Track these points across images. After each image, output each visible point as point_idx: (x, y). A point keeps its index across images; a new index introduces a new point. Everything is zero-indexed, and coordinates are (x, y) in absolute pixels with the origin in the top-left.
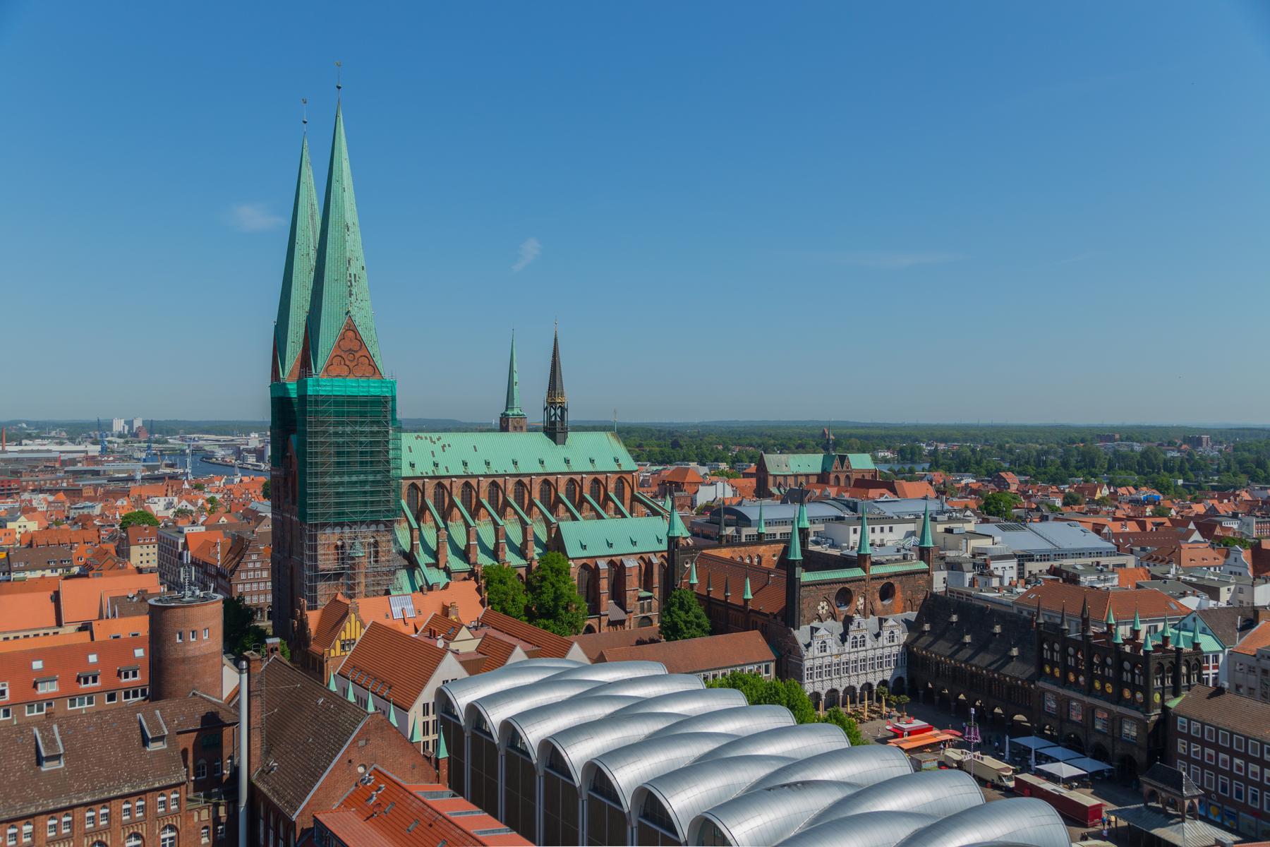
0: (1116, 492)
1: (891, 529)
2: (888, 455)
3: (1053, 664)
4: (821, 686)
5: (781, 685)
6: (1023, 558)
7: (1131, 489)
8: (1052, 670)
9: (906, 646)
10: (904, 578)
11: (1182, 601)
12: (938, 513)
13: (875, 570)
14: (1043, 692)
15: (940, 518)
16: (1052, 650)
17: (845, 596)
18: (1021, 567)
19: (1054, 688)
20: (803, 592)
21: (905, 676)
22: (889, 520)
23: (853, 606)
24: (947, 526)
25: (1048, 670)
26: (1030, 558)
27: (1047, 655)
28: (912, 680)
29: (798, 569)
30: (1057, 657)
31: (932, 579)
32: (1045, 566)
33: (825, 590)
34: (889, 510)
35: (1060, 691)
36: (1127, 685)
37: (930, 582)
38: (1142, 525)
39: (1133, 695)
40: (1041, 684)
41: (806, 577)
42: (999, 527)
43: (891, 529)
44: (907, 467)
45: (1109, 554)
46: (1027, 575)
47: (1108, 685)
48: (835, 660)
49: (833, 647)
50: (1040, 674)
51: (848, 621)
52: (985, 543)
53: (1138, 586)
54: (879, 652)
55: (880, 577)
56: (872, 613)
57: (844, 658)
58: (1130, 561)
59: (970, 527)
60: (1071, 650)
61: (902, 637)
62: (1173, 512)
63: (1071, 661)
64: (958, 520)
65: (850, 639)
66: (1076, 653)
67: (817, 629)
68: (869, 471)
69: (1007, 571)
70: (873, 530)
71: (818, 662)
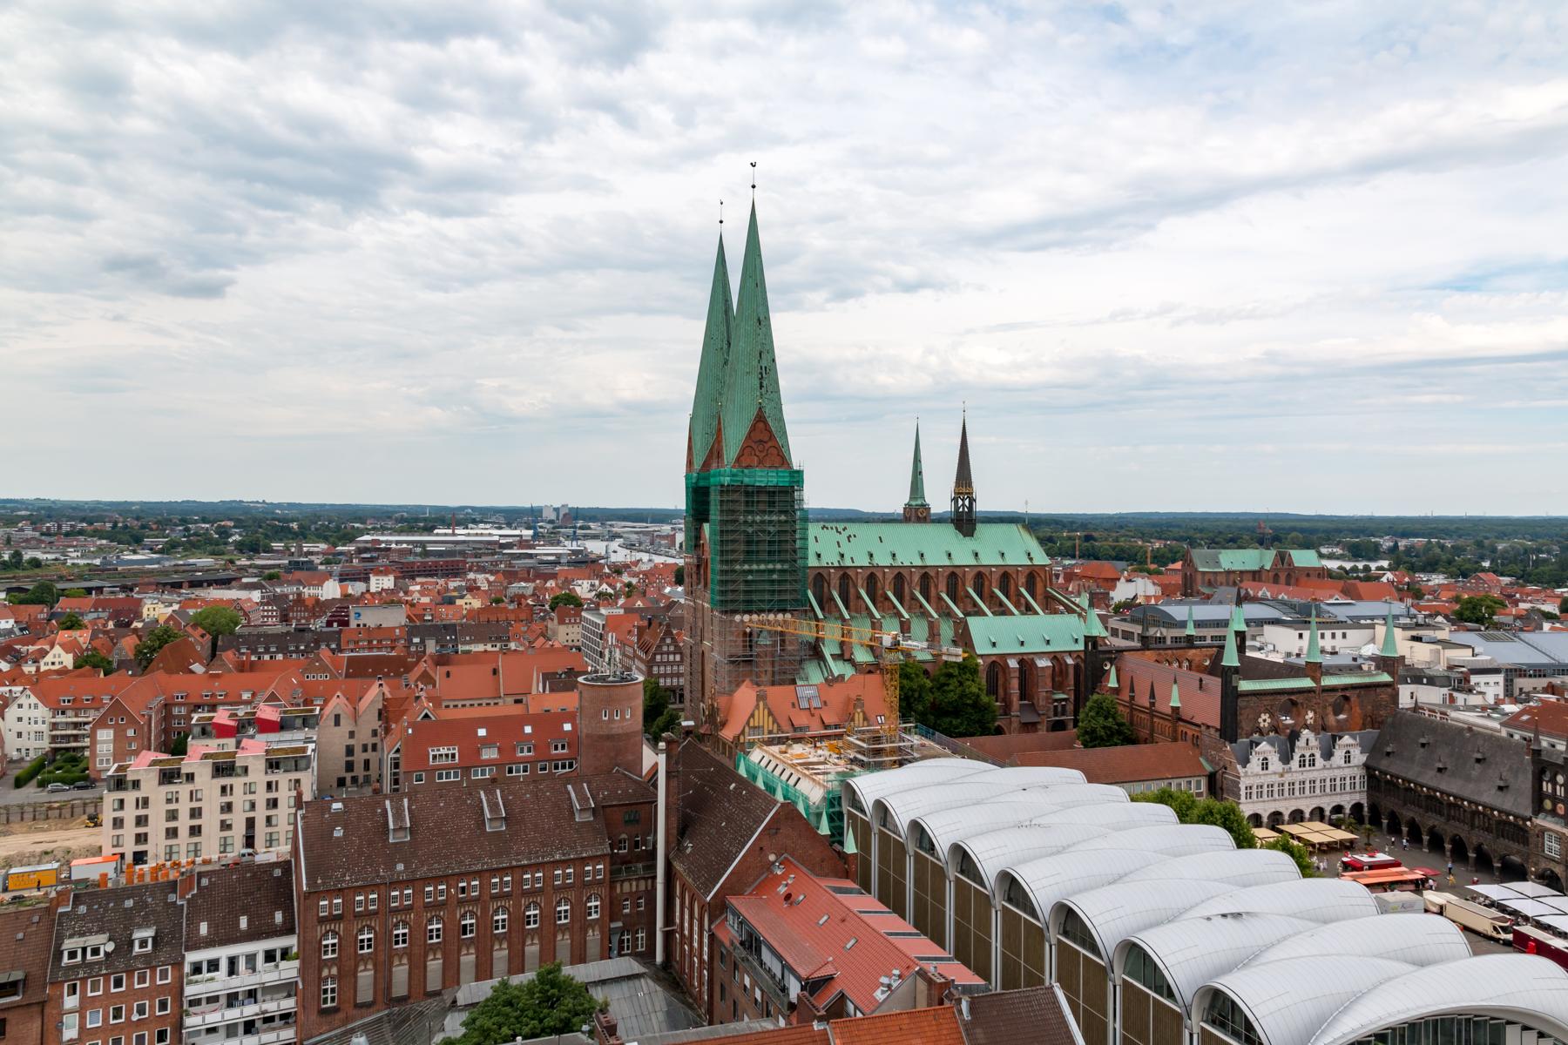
1: (1344, 636)
5: (1214, 806)
6: (1513, 673)
9: (1367, 766)
13: (1328, 681)
14: (1543, 830)
16: (1554, 782)
18: (1509, 684)
19: (1558, 828)
20: (1241, 702)
21: (1365, 802)
22: (1339, 624)
24: (1414, 633)
27: (1547, 787)
28: (1374, 807)
32: (1544, 682)
33: (1267, 701)
34: (1341, 613)
41: (1245, 686)
42: (1482, 636)
43: (1344, 636)
44: (1360, 565)
46: (1517, 692)
49: (1275, 764)
50: (1538, 809)
51: (1294, 736)
52: (1463, 656)
55: (1333, 689)
56: (1324, 729)
57: (1288, 778)
59: (1443, 635)
61: (1359, 758)
65: (1296, 757)
67: (1258, 744)
69: (1492, 687)
70: (1323, 636)
71: (1258, 781)
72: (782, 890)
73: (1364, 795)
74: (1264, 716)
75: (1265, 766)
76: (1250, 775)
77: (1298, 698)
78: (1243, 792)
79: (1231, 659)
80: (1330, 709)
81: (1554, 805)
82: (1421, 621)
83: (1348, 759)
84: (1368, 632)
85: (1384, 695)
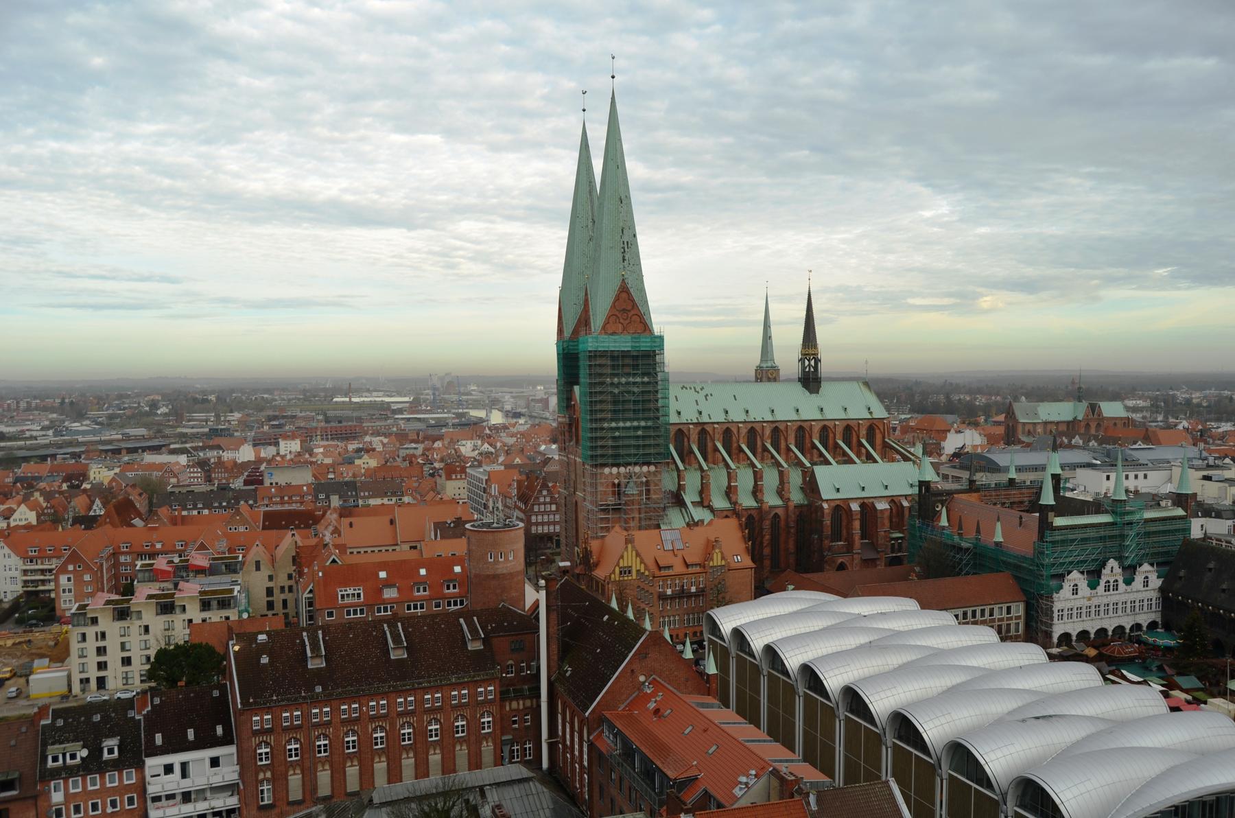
1: (1145, 476)
2: (1141, 403)
4: (1074, 629)
9: (1161, 589)
21: (1159, 620)
24: (1205, 473)
29: (1051, 514)
37: (1187, 530)
41: (1059, 521)
43: (1145, 476)
48: (1088, 603)
54: (1132, 597)
57: (1095, 601)
61: (1156, 582)
64: (1216, 467)
65: (1102, 583)
68: (1121, 418)
70: (1127, 477)
71: (1069, 605)
72: (652, 706)
73: (1159, 615)
75: (1075, 591)
76: (1063, 599)
78: (1056, 615)
79: (1048, 498)
82: (1211, 463)
83: (1146, 584)
84: (1165, 473)
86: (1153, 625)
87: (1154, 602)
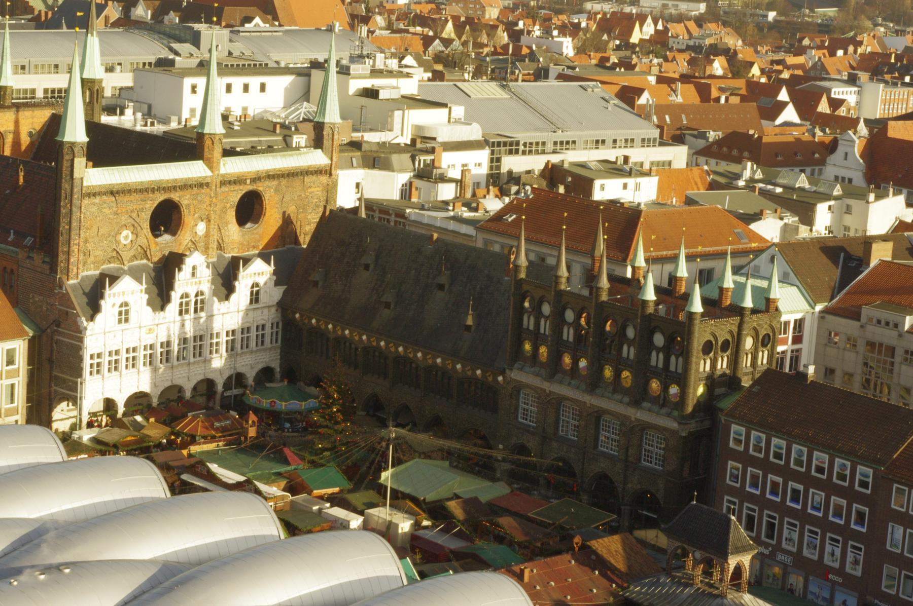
0: (666, 30)
1: (263, 88)
3: (537, 338)
7: (691, 25)
8: (535, 349)
9: (283, 306)
10: (284, 182)
11: (754, 227)
12: (353, 59)
14: (518, 388)
15: (355, 69)
16: (538, 314)
17: (166, 217)
18: (495, 161)
19: (536, 382)
21: (276, 365)
23: (184, 238)
24: (368, 83)
25: (527, 347)
26: (513, 148)
27: (529, 322)
29: (80, 162)
30: (545, 327)
31: (335, 185)
33: (130, 203)
35: (547, 386)
36: (656, 373)
37: (331, 191)
38: (704, 92)
39: (665, 388)
40: (516, 375)
43: (263, 88)
45: (646, 142)
47: (625, 374)
53: (689, 201)
55: (238, 181)
58: (678, 156)
60: (569, 315)
62: (755, 71)
63: (568, 334)
64: (390, 73)
65: (175, 296)
66: (578, 317)
74: (125, 233)
75: (124, 316)
76: (99, 335)
77: (183, 199)
78: (87, 362)
80: (231, 215)
81: (535, 349)
82: (380, 65)
85: (315, 187)
86: (266, 374)
87: (268, 331)
